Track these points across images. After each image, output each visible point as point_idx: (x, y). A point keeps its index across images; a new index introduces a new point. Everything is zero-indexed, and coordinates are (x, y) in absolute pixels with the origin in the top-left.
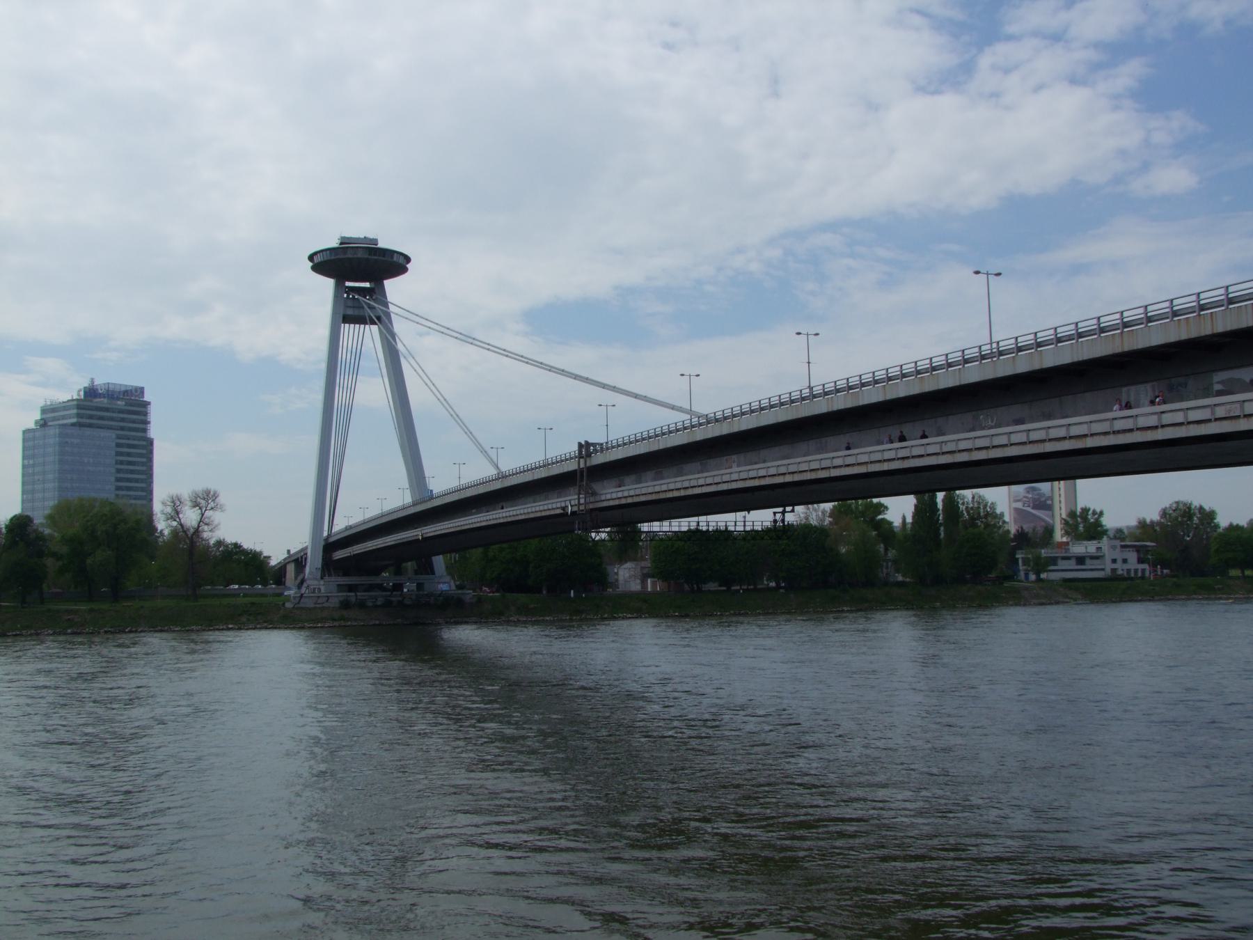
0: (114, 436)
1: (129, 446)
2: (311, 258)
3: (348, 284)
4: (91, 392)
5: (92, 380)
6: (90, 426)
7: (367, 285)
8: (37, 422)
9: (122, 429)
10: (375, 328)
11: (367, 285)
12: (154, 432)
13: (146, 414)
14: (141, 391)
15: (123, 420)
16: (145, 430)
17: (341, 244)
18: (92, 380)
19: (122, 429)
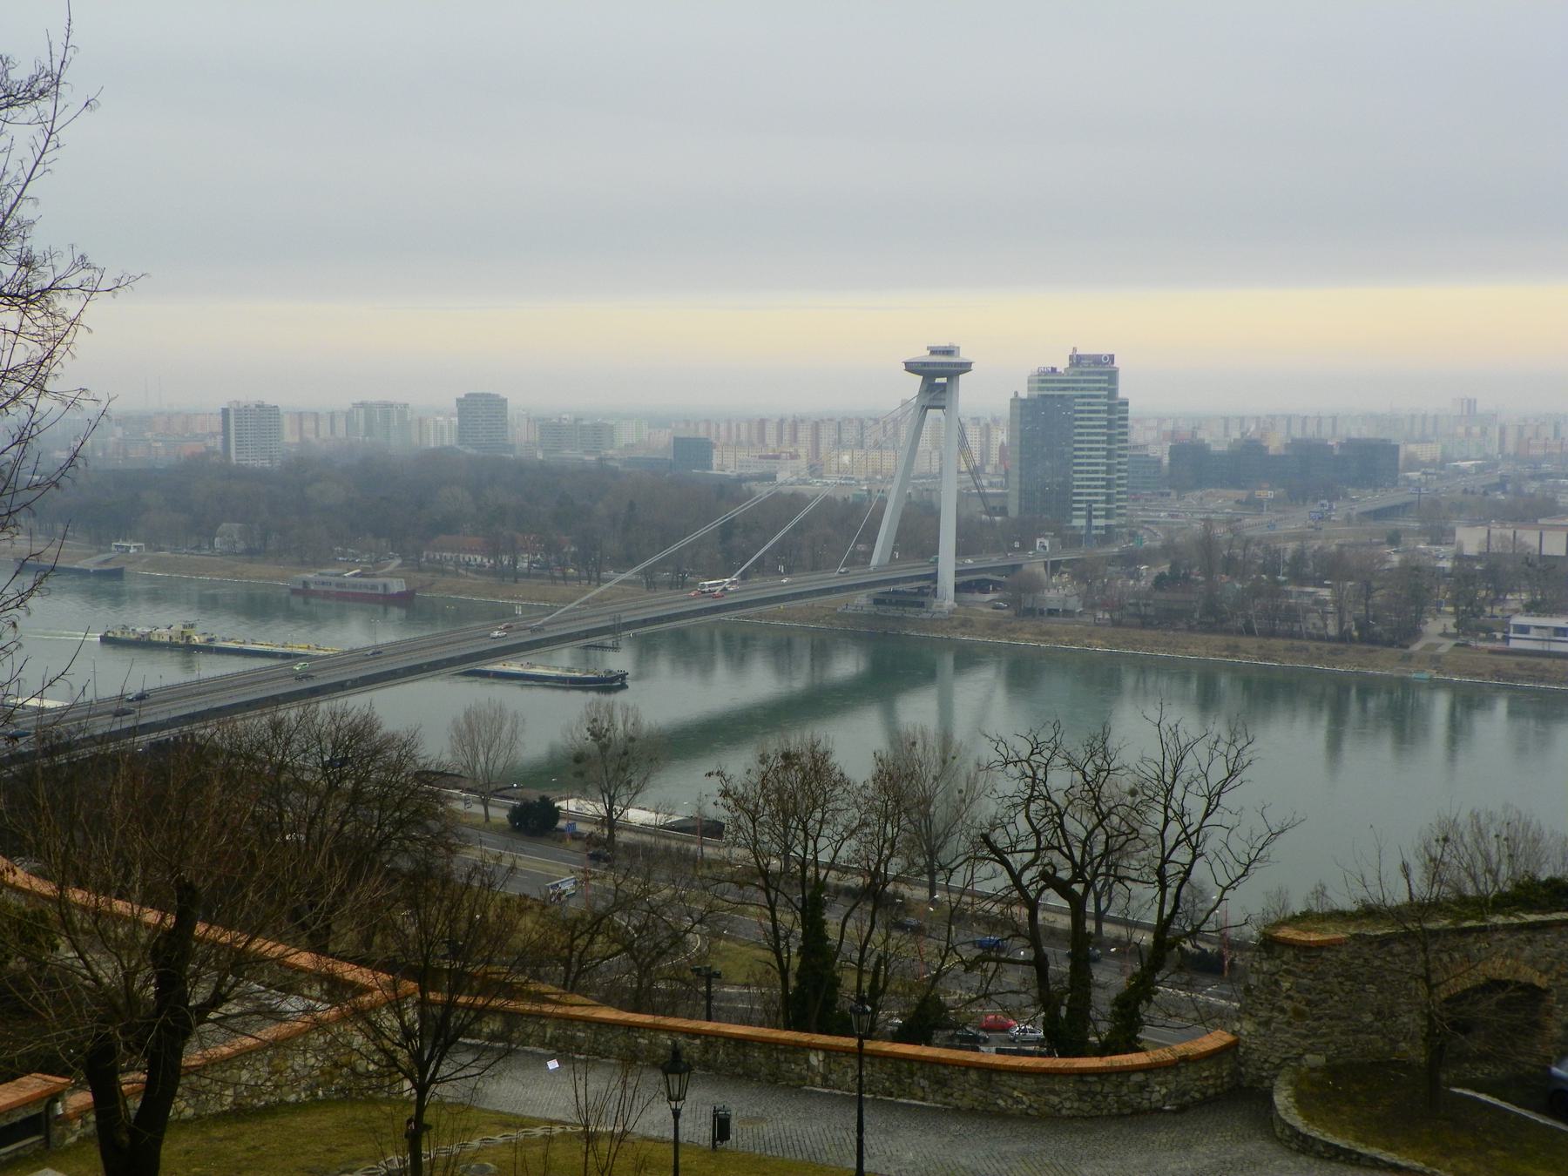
2: (906, 364)
5: (1075, 349)
7: (944, 380)
9: (1083, 397)
11: (944, 380)
12: (1122, 394)
14: (1112, 357)
18: (1075, 349)
19: (1083, 397)
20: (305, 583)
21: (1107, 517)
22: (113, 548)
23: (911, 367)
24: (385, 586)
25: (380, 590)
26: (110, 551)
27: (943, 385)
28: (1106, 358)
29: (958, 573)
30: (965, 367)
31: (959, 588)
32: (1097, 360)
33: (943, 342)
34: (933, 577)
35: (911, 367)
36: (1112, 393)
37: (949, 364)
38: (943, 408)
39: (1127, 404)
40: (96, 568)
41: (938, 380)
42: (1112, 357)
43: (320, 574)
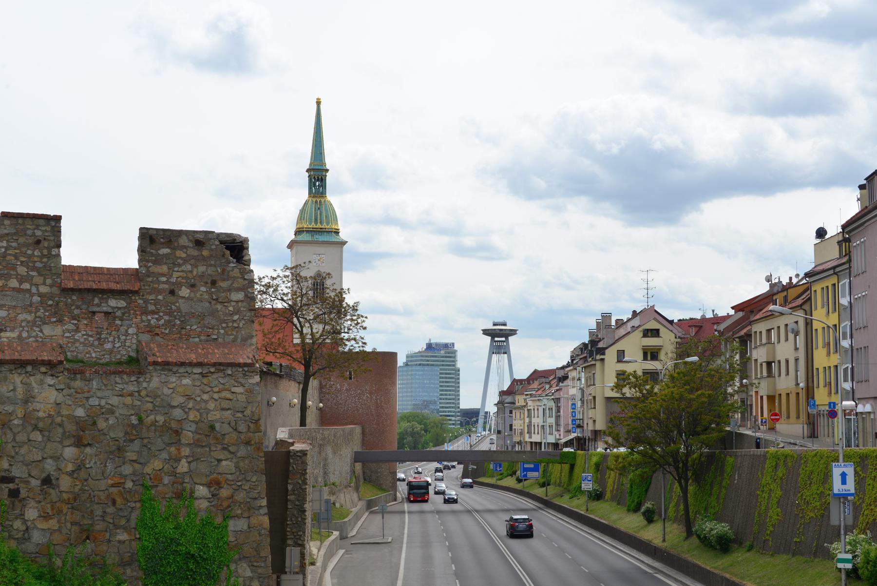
0: (439, 369)
1: (446, 374)
3: (496, 339)
4: (429, 346)
5: (430, 340)
6: (428, 365)
8: (404, 363)
9: (443, 365)
10: (506, 355)
11: (503, 339)
12: (459, 365)
13: (455, 357)
14: (453, 344)
15: (443, 361)
16: (454, 365)
17: (495, 325)
18: (430, 340)
19: (443, 365)
23: (486, 332)
27: (504, 341)
30: (513, 332)
32: (446, 346)
35: (486, 332)
37: (505, 330)
38: (506, 353)
39: (459, 370)
42: (453, 344)
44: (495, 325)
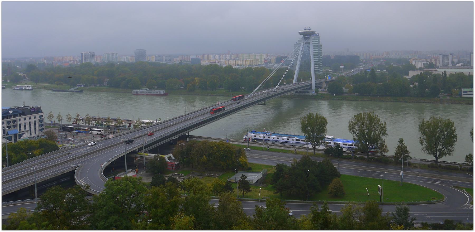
7: (309, 36)
11: (309, 36)
12: (322, 42)
20: (137, 92)
21: (319, 72)
22: (77, 86)
23: (300, 33)
24: (160, 92)
25: (159, 93)
26: (77, 87)
28: (317, 35)
29: (316, 84)
31: (316, 87)
33: (308, 27)
34: (311, 85)
36: (319, 42)
39: (322, 45)
40: (76, 90)
41: (306, 36)
43: (142, 90)
44: (305, 30)
